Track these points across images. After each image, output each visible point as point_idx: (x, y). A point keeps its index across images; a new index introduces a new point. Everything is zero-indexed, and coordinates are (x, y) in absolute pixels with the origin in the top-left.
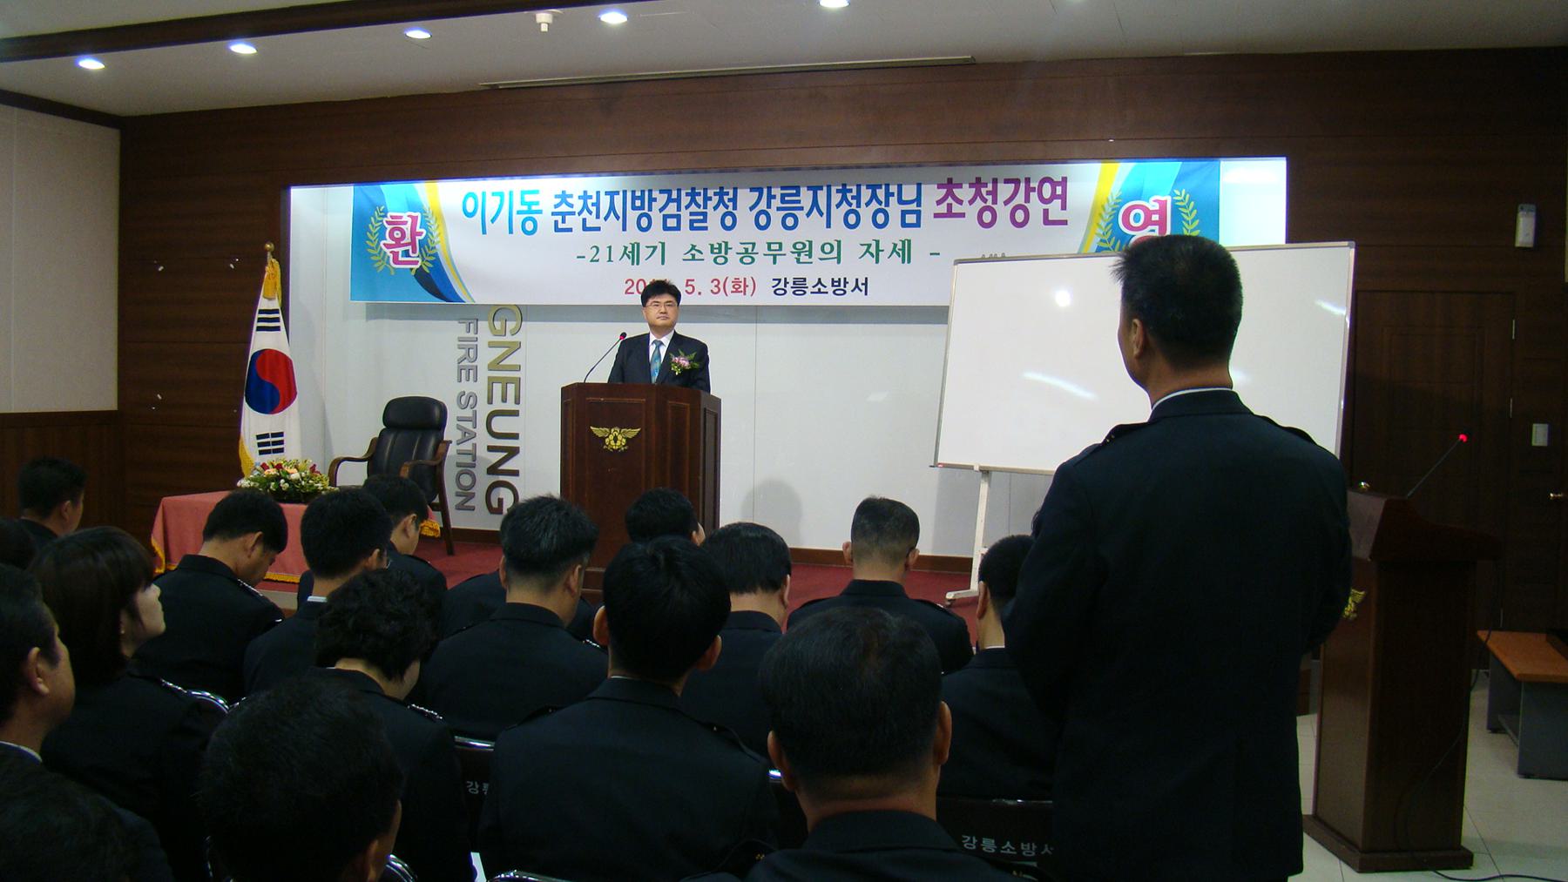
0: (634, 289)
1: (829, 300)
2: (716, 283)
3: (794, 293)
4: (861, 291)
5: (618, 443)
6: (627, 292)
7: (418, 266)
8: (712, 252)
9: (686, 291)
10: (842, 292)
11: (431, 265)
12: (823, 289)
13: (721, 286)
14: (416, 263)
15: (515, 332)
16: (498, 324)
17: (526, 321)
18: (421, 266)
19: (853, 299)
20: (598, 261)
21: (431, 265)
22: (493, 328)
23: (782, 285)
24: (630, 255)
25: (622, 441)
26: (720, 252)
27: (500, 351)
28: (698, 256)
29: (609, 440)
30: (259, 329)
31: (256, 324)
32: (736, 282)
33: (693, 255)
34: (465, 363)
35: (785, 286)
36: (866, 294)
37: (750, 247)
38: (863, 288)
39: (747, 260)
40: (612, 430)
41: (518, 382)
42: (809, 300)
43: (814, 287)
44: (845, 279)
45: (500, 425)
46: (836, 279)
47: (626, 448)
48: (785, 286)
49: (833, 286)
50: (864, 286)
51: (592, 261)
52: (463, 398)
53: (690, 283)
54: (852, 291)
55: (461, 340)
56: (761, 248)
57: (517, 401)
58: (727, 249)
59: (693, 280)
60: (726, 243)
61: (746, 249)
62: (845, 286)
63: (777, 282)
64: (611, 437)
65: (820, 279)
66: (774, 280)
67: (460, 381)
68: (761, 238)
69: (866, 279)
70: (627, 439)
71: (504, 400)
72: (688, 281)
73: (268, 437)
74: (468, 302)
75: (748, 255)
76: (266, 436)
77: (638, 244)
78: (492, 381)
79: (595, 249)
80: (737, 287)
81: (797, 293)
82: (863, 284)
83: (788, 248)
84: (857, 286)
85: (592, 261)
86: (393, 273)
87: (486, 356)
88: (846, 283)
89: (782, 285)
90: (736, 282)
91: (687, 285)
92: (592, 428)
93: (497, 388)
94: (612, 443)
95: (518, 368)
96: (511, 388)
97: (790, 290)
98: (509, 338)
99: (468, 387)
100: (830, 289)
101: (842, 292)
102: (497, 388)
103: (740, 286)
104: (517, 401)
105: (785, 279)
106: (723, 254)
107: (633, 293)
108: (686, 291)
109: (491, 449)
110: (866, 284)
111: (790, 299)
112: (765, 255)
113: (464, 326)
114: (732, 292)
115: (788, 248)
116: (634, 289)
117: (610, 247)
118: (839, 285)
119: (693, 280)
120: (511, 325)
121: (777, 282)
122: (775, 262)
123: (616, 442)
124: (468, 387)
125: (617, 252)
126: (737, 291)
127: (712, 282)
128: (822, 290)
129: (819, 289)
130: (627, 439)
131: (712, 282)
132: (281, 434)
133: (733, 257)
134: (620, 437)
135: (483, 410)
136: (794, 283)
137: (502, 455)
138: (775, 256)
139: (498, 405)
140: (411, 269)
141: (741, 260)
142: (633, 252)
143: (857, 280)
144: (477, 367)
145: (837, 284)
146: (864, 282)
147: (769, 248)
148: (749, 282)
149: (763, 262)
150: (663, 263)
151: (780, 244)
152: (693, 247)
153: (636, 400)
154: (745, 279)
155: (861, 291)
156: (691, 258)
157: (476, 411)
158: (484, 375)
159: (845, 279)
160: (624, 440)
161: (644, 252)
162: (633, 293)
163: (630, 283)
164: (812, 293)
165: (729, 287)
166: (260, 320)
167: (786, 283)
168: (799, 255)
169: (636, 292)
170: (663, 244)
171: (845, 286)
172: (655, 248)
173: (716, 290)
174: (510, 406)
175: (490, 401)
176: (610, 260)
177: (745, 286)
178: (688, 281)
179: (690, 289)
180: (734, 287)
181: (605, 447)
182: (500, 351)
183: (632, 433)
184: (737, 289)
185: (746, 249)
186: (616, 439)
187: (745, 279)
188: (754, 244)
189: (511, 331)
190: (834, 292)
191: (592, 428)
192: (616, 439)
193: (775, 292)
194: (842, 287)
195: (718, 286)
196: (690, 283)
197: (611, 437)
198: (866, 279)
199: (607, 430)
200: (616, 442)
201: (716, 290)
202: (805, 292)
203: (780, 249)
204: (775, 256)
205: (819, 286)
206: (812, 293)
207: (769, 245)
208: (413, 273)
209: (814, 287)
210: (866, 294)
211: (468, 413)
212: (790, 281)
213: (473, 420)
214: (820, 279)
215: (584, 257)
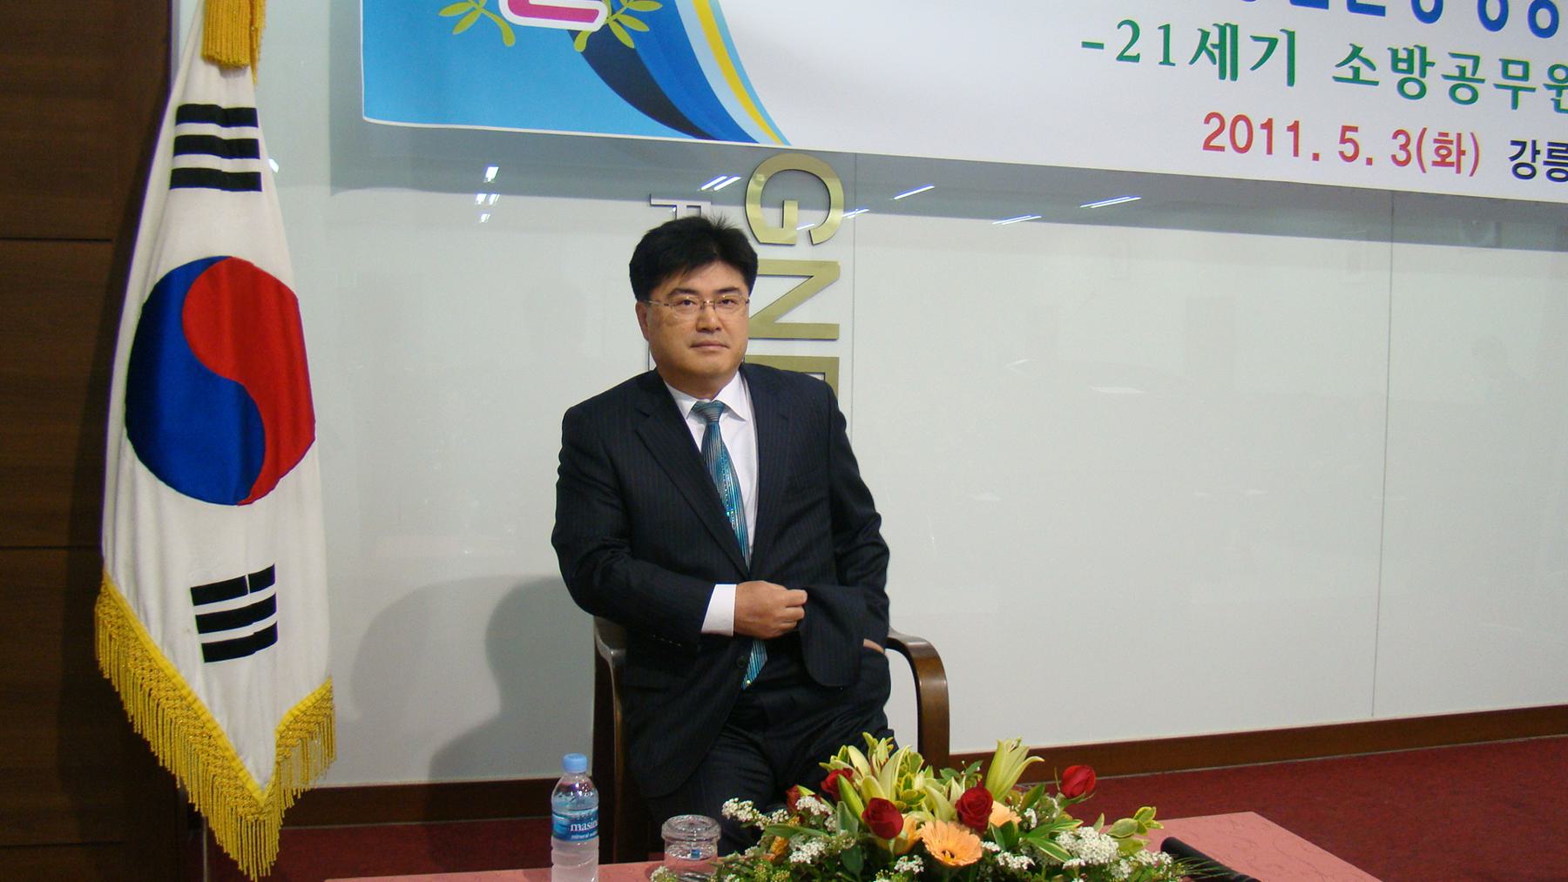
0: (1223, 139)
2: (1402, 139)
6: (1207, 146)
7: (595, 26)
8: (1395, 69)
9: (1342, 154)
11: (643, 28)
13: (1412, 148)
14: (590, 15)
18: (606, 28)
20: (1136, 59)
21: (643, 28)
23: (1526, 157)
24: (1216, 52)
26: (1410, 70)
28: (1365, 73)
30: (182, 179)
31: (163, 161)
32: (1442, 141)
33: (1356, 71)
35: (1534, 160)
37: (1468, 64)
39: (1463, 94)
48: (1534, 160)
51: (1121, 58)
53: (1349, 135)
56: (1490, 71)
58: (1425, 64)
59: (1355, 129)
60: (1423, 51)
61: (1462, 69)
63: (1518, 148)
66: (1514, 143)
68: (1492, 48)
72: (1346, 129)
73: (243, 593)
74: (765, 141)
75: (1464, 83)
76: (233, 588)
77: (1234, 29)
79: (1128, 30)
80: (1443, 152)
81: (1554, 175)
83: (1538, 77)
85: (1121, 58)
86: (510, 40)
90: (1442, 141)
91: (1343, 141)
95: (826, 333)
97: (1542, 170)
103: (1449, 154)
105: (1534, 143)
106: (1416, 74)
107: (1221, 149)
108: (1342, 154)
112: (1498, 86)
114: (1435, 164)
115: (1538, 77)
116: (1223, 139)
117: (1166, 29)
119: (1355, 129)
121: (1518, 148)
122: (1515, 105)
125: (1183, 46)
126: (1443, 163)
127: (1395, 136)
131: (1395, 136)
132: (264, 578)
133: (1436, 84)
136: (1550, 151)
138: (1515, 90)
140: (574, 34)
141: (1453, 90)
142: (1221, 46)
147: (1505, 74)
149: (1493, 98)
150: (1291, 81)
151: (1526, 65)
152: (1356, 52)
154: (1459, 136)
156: (1351, 76)
161: (1249, 52)
162: (1221, 149)
163: (1215, 123)
165: (1429, 155)
166: (184, 145)
167: (1535, 152)
168: (1560, 94)
169: (1229, 147)
170: (1291, 36)
172: (1273, 43)
173: (1402, 156)
176: (1166, 61)
177: (1461, 153)
178: (1346, 129)
179: (1349, 150)
180: (1437, 150)
184: (1444, 157)
185: (1462, 69)
187: (1459, 136)
188: (1476, 60)
195: (1407, 149)
196: (1349, 135)
201: (1402, 156)
203: (1525, 77)
204: (1515, 90)
207: (1506, 63)
208: (580, 44)
212: (1543, 147)
215: (1100, 46)
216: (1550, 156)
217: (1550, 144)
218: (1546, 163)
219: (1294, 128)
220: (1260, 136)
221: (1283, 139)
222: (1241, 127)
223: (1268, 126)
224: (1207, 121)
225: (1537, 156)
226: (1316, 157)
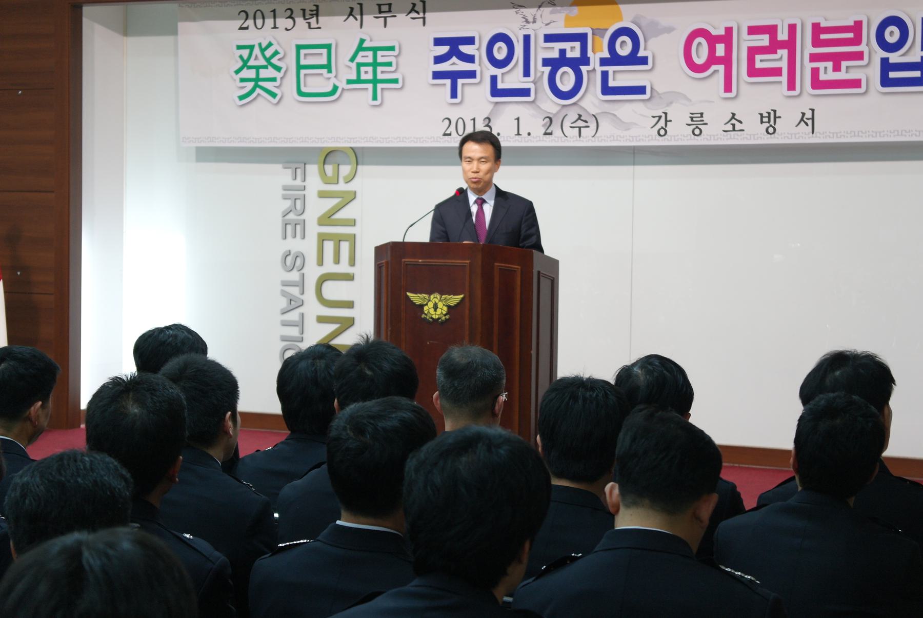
5: (439, 311)
15: (348, 181)
16: (329, 169)
17: (363, 164)
22: (323, 174)
25: (442, 310)
27: (332, 203)
29: (429, 309)
34: (291, 216)
40: (432, 297)
41: (352, 239)
45: (333, 291)
47: (447, 317)
52: (289, 260)
55: (286, 188)
57: (352, 262)
64: (431, 305)
67: (285, 238)
70: (449, 307)
71: (337, 261)
78: (322, 238)
87: (316, 207)
92: (409, 294)
93: (329, 246)
94: (432, 311)
95: (353, 223)
96: (345, 247)
98: (342, 187)
99: (294, 245)
102: (329, 246)
104: (352, 262)
109: (322, 320)
113: (289, 171)
120: (345, 170)
123: (435, 310)
124: (294, 245)
130: (449, 307)
134: (440, 305)
135: (313, 273)
137: (333, 327)
139: (329, 267)
144: (304, 220)
153: (458, 262)
157: (303, 274)
158: (313, 230)
160: (445, 309)
174: (343, 267)
175: (321, 262)
181: (423, 316)
182: (332, 203)
183: (455, 299)
186: (436, 307)
189: (345, 178)
191: (409, 294)
192: (436, 307)
197: (431, 305)
199: (426, 296)
200: (435, 310)
211: (294, 276)
213: (301, 284)
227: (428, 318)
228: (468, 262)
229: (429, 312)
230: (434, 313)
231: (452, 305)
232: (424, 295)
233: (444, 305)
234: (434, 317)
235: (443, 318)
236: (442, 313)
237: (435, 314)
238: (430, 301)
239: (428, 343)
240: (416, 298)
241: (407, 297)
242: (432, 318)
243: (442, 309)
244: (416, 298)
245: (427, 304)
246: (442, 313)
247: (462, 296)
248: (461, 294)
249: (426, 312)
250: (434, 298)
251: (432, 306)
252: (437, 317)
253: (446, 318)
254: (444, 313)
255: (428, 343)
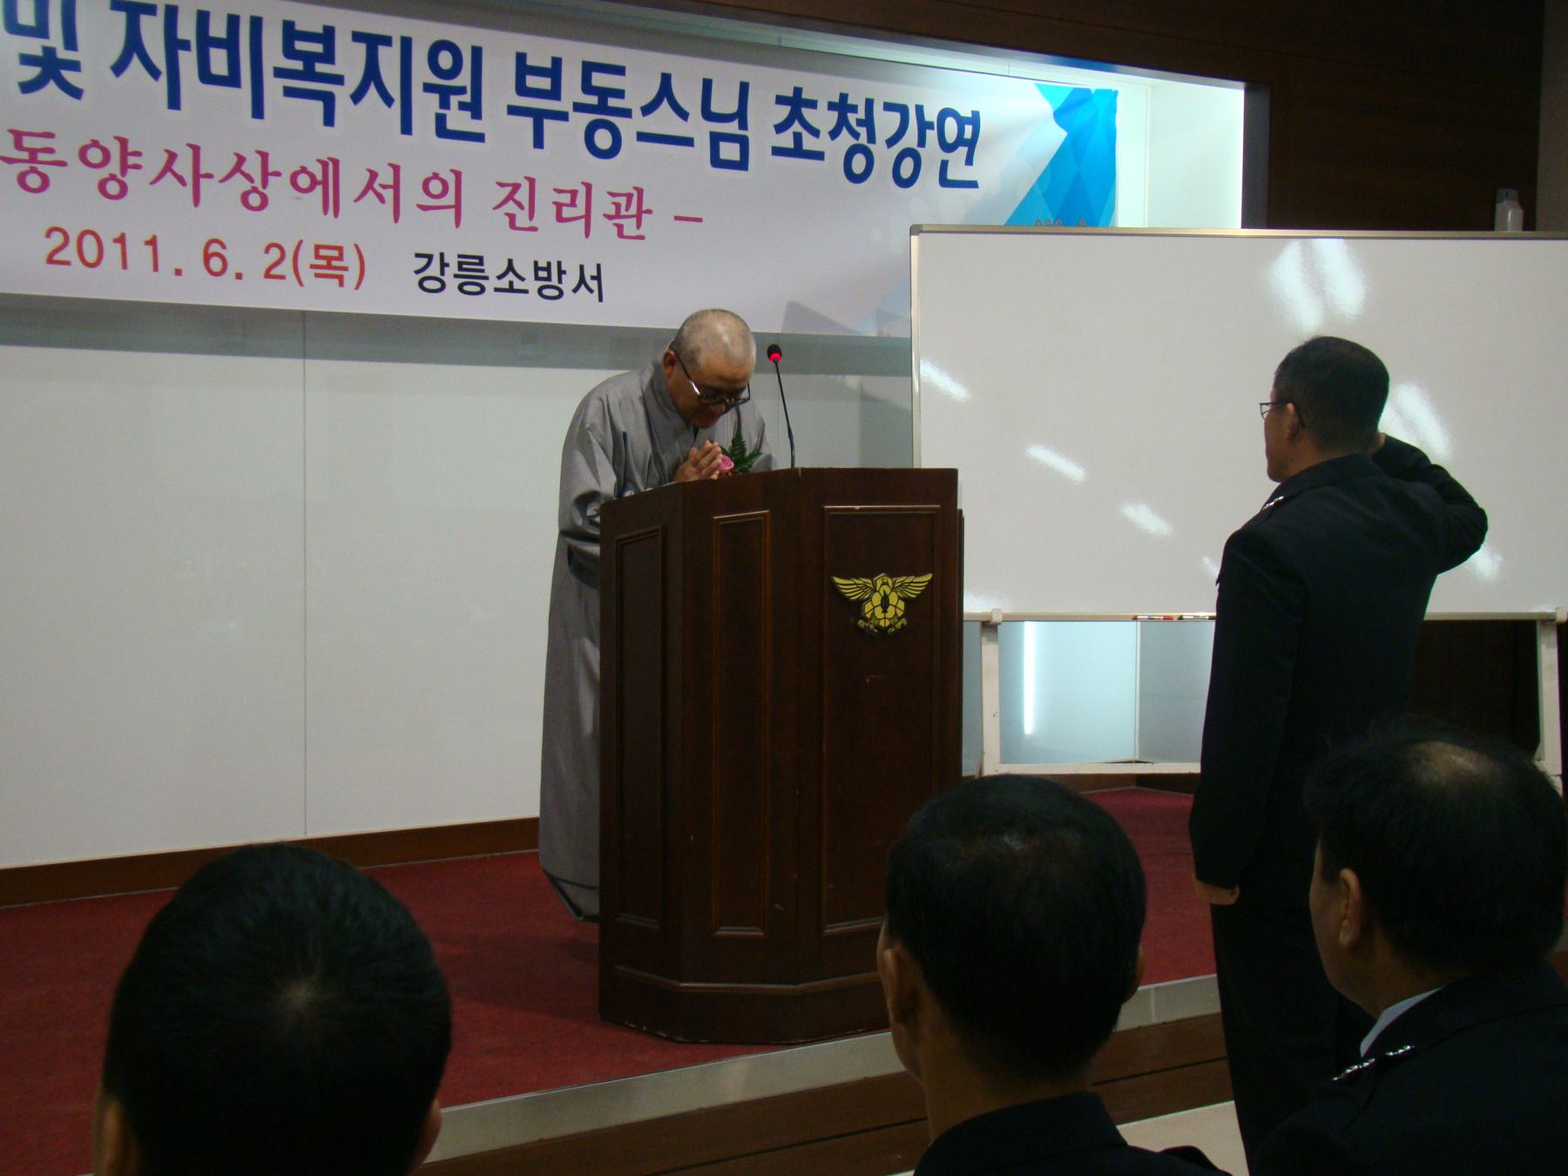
0: (70, 253)
1: (529, 309)
3: (461, 288)
4: (591, 291)
5: (891, 612)
6: (50, 260)
10: (555, 293)
12: (518, 284)
19: (576, 310)
23: (434, 270)
25: (897, 607)
29: (872, 607)
35: (442, 273)
36: (601, 299)
38: (593, 284)
42: (491, 307)
43: (500, 277)
44: (559, 264)
46: (543, 264)
47: (904, 621)
48: (442, 273)
49: (537, 278)
50: (596, 282)
54: (575, 290)
62: (560, 281)
63: (424, 261)
65: (510, 261)
66: (418, 255)
69: (599, 266)
70: (907, 600)
81: (467, 288)
82: (593, 278)
84: (582, 281)
88: (561, 272)
89: (434, 270)
92: (837, 580)
94: (879, 612)
97: (452, 284)
100: (532, 285)
101: (555, 293)
105: (442, 255)
107: (67, 263)
110: (598, 278)
111: (452, 305)
116: (70, 253)
118: (549, 278)
121: (424, 261)
123: (885, 611)
128: (515, 287)
129: (511, 283)
134: (893, 598)
136: (460, 265)
143: (582, 267)
145: (543, 274)
146: (595, 274)
148: (350, 259)
155: (591, 291)
159: (559, 264)
160: (901, 605)
162: (67, 263)
163: (57, 239)
164: (497, 290)
167: (443, 265)
169: (74, 258)
171: (560, 281)
181: (861, 623)
186: (885, 603)
190: (540, 291)
191: (837, 580)
192: (885, 603)
193: (421, 284)
194: (554, 282)
197: (877, 599)
198: (599, 266)
200: (885, 611)
202: (483, 290)
205: (511, 276)
206: (497, 290)
209: (500, 277)
210: (601, 299)
212: (453, 261)
214: (510, 261)
216: (460, 268)
217: (460, 256)
218: (456, 276)
219: (152, 242)
220: (113, 251)
221: (139, 254)
222: (89, 242)
223: (121, 240)
224: (48, 234)
225: (446, 269)
226: (178, 272)
227: (872, 626)
228: (938, 506)
229: (873, 614)
230: (882, 616)
231: (914, 596)
232: (865, 580)
233: (899, 598)
234: (882, 623)
235: (899, 625)
236: (896, 614)
237: (885, 618)
238: (875, 590)
239: (868, 680)
240: (848, 586)
241: (834, 588)
242: (878, 627)
243: (895, 606)
244: (848, 586)
245: (869, 599)
246: (896, 614)
247: (929, 577)
248: (924, 574)
249: (868, 616)
250: (883, 584)
251: (879, 603)
252: (888, 623)
253: (902, 625)
254: (900, 613)
255: (868, 680)
